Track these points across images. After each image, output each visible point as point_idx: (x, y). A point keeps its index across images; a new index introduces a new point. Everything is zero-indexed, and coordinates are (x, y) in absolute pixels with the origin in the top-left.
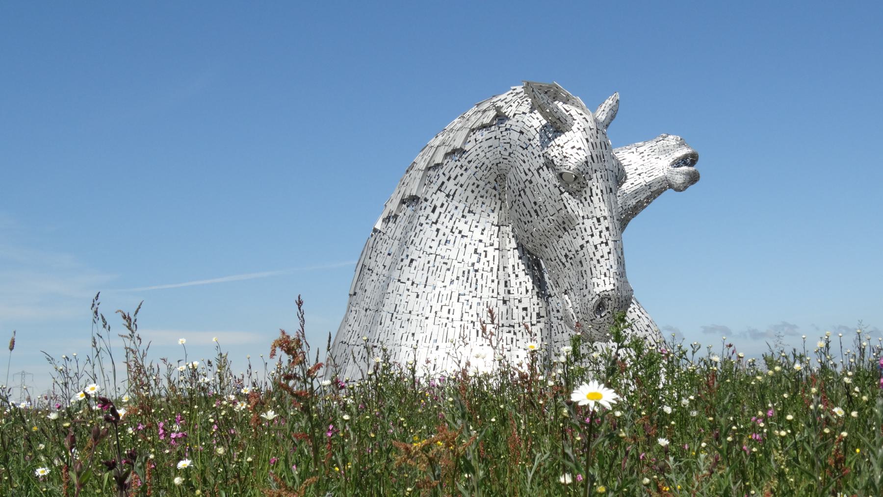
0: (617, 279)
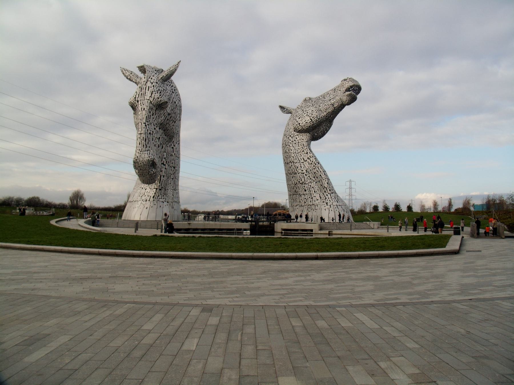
0: (138, 153)
